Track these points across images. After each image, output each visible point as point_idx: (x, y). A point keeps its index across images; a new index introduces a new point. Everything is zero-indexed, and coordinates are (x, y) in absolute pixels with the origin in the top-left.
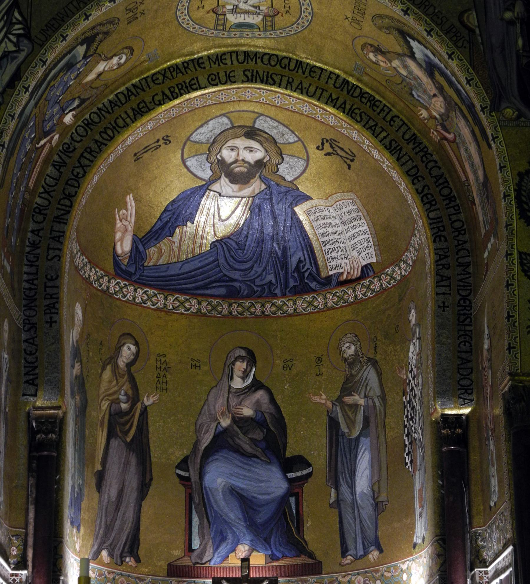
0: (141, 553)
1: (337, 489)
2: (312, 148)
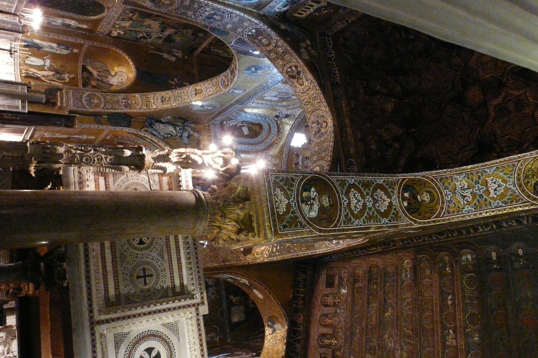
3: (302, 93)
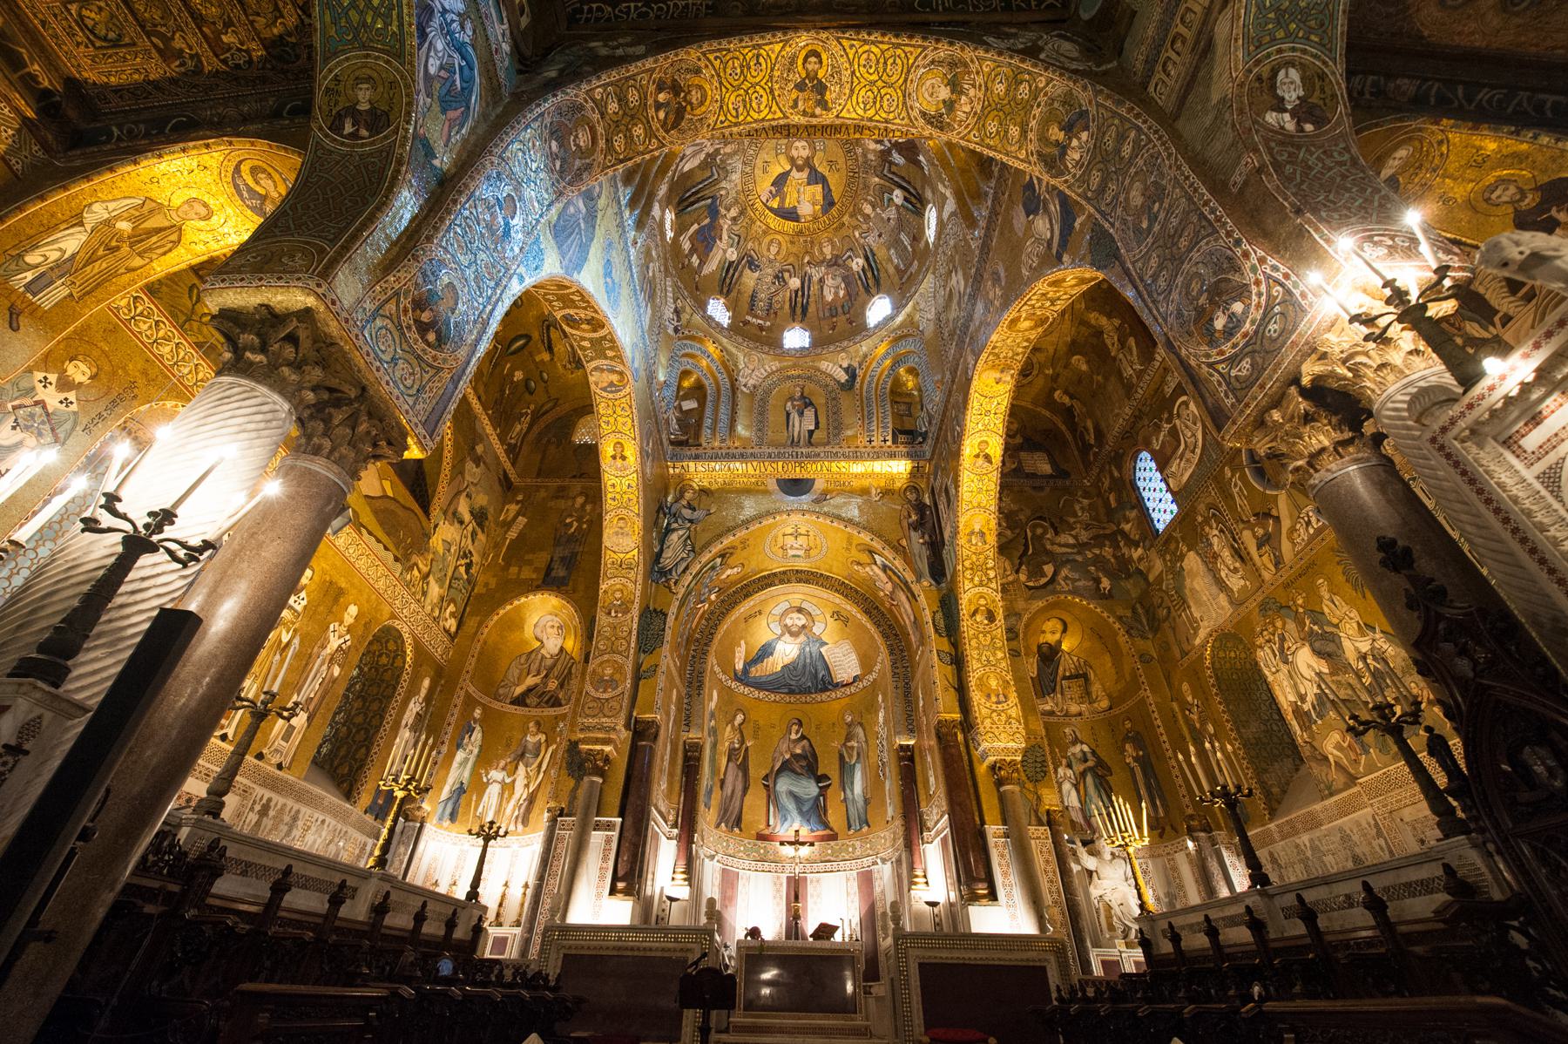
2: (828, 616)
3: (721, 107)
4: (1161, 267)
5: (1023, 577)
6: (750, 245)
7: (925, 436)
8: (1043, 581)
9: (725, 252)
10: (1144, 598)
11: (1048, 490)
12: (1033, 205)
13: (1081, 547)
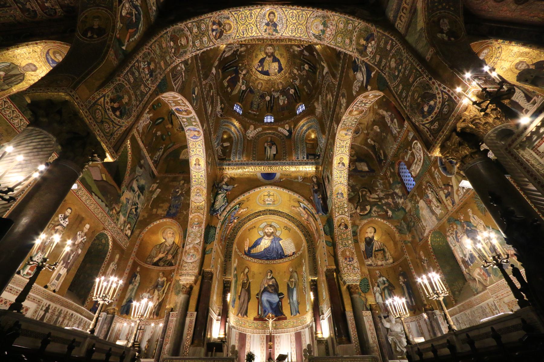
0: (248, 314)
1: (289, 299)
2: (282, 228)
3: (237, 31)
4: (403, 89)
5: (358, 211)
6: (251, 84)
7: (319, 156)
8: (366, 212)
9: (241, 86)
10: (404, 219)
11: (367, 177)
12: (356, 68)
13: (380, 199)
